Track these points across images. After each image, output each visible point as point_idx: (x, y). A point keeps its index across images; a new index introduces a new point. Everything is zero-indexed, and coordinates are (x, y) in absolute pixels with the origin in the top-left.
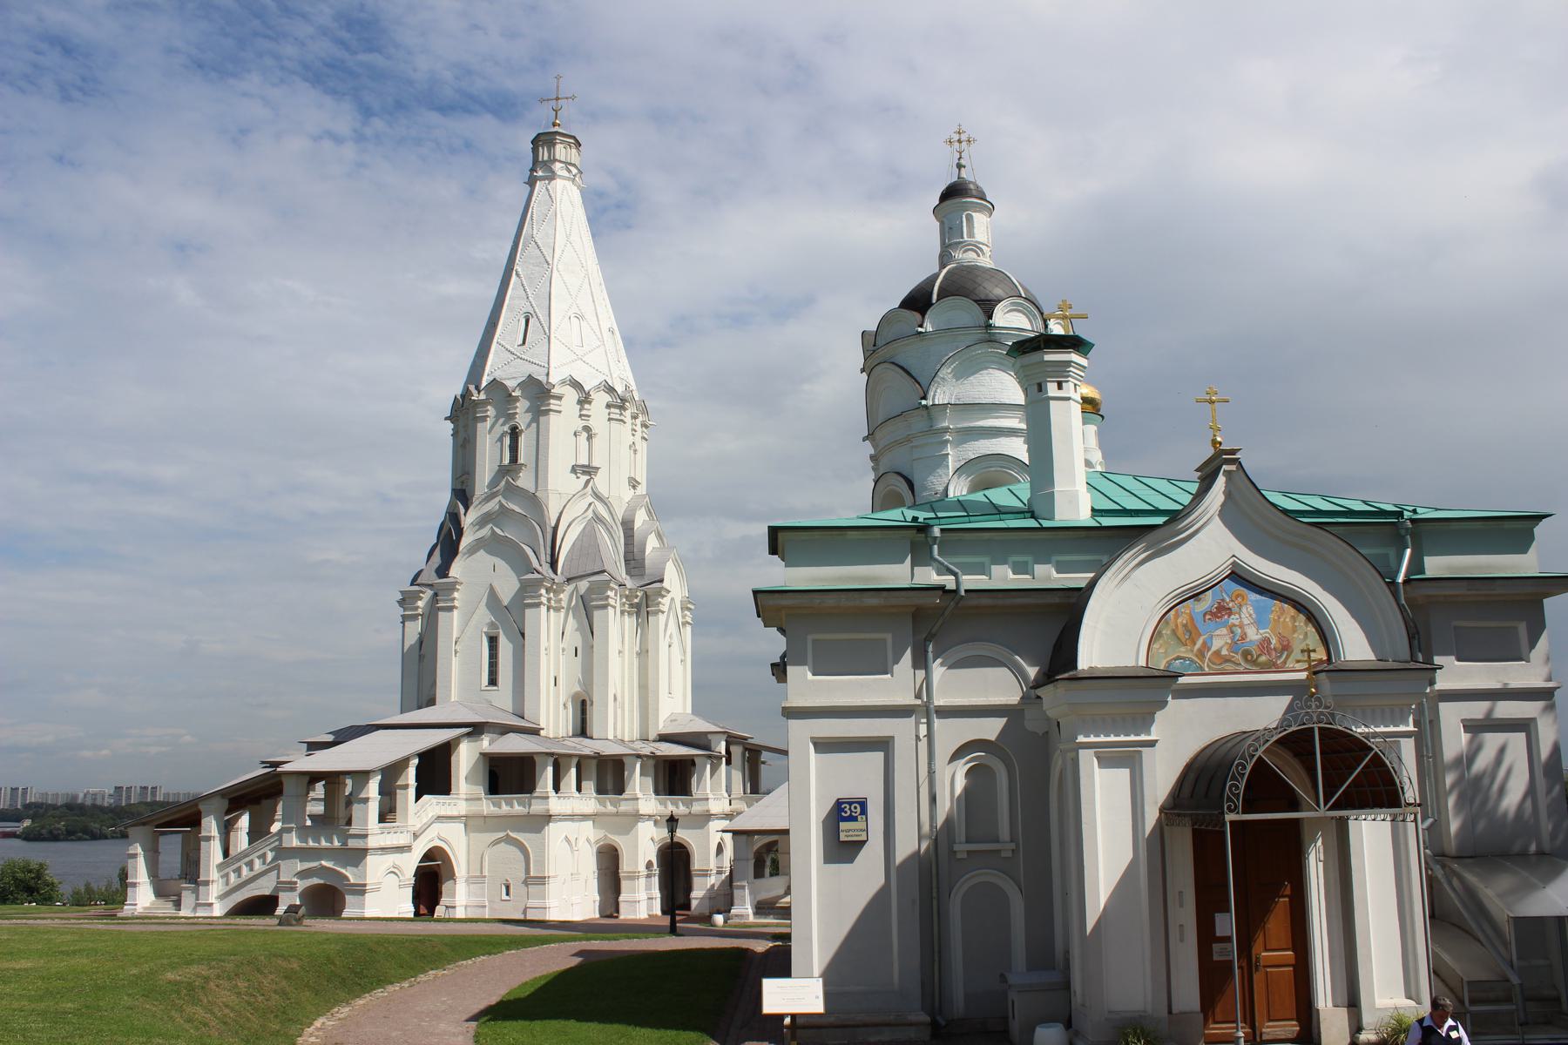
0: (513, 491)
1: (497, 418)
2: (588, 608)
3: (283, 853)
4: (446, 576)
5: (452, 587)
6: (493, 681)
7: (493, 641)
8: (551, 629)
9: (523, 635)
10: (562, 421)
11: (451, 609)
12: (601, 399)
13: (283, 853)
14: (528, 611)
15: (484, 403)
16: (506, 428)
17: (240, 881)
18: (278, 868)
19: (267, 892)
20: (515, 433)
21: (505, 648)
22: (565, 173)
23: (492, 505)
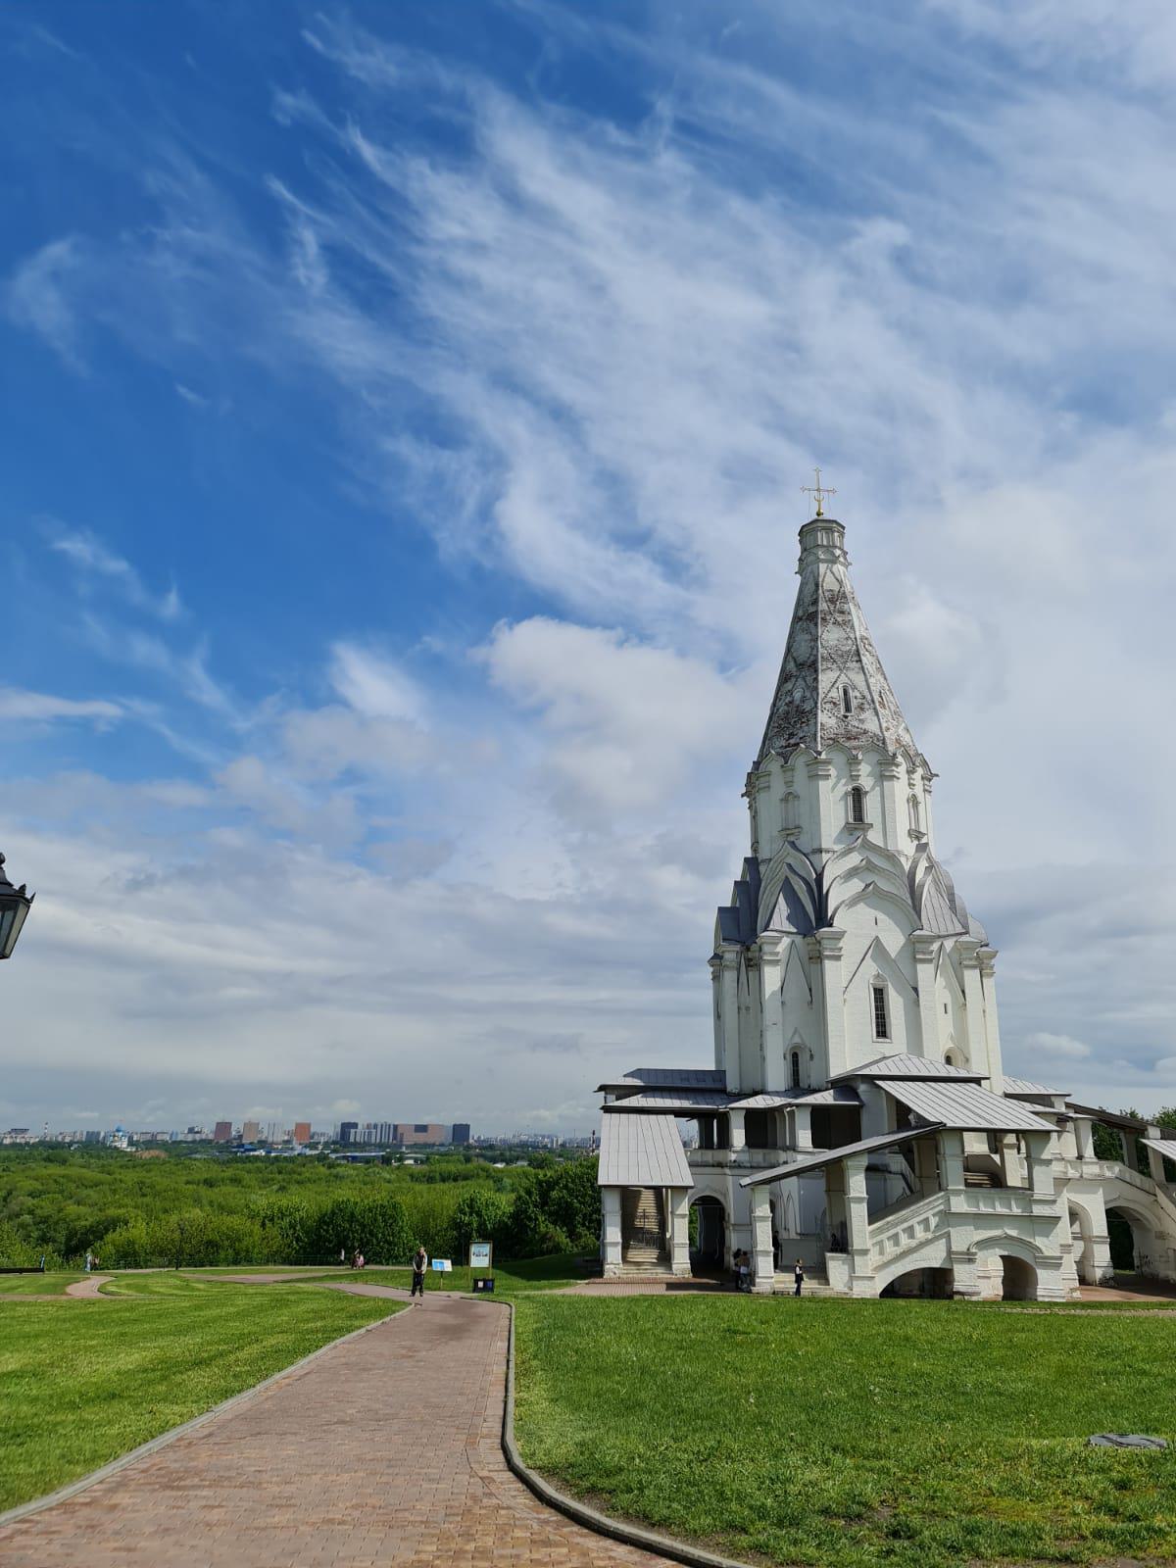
0: (868, 846)
1: (839, 778)
2: (959, 967)
3: (948, 1217)
4: (831, 925)
5: (840, 935)
6: (882, 1031)
7: (879, 994)
8: (934, 985)
9: (916, 990)
10: (900, 789)
11: (838, 958)
12: (920, 771)
13: (948, 1217)
14: (920, 967)
15: (827, 762)
16: (850, 788)
17: (899, 1250)
18: (948, 1236)
19: (936, 1264)
20: (857, 795)
21: (895, 1003)
22: (841, 559)
23: (854, 859)
